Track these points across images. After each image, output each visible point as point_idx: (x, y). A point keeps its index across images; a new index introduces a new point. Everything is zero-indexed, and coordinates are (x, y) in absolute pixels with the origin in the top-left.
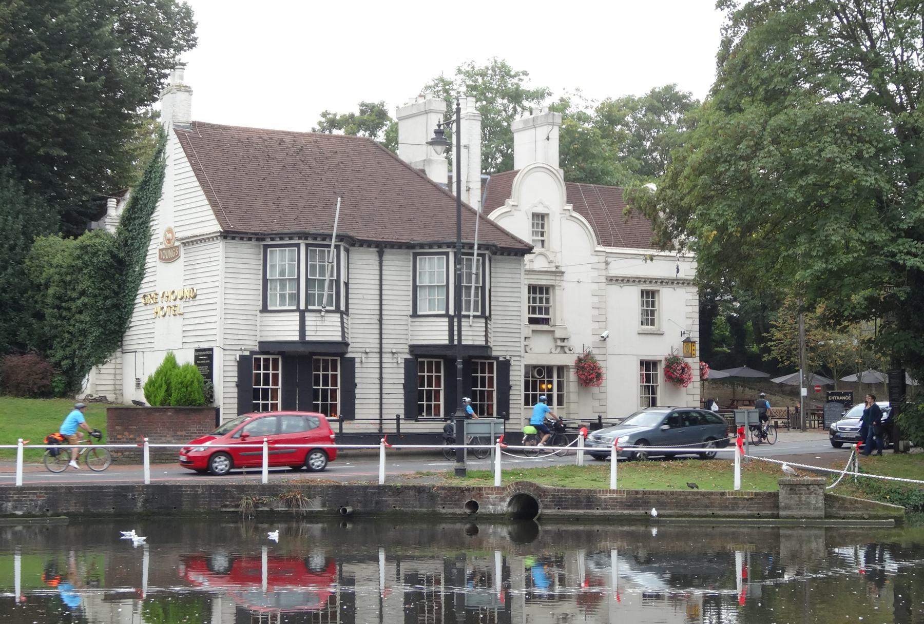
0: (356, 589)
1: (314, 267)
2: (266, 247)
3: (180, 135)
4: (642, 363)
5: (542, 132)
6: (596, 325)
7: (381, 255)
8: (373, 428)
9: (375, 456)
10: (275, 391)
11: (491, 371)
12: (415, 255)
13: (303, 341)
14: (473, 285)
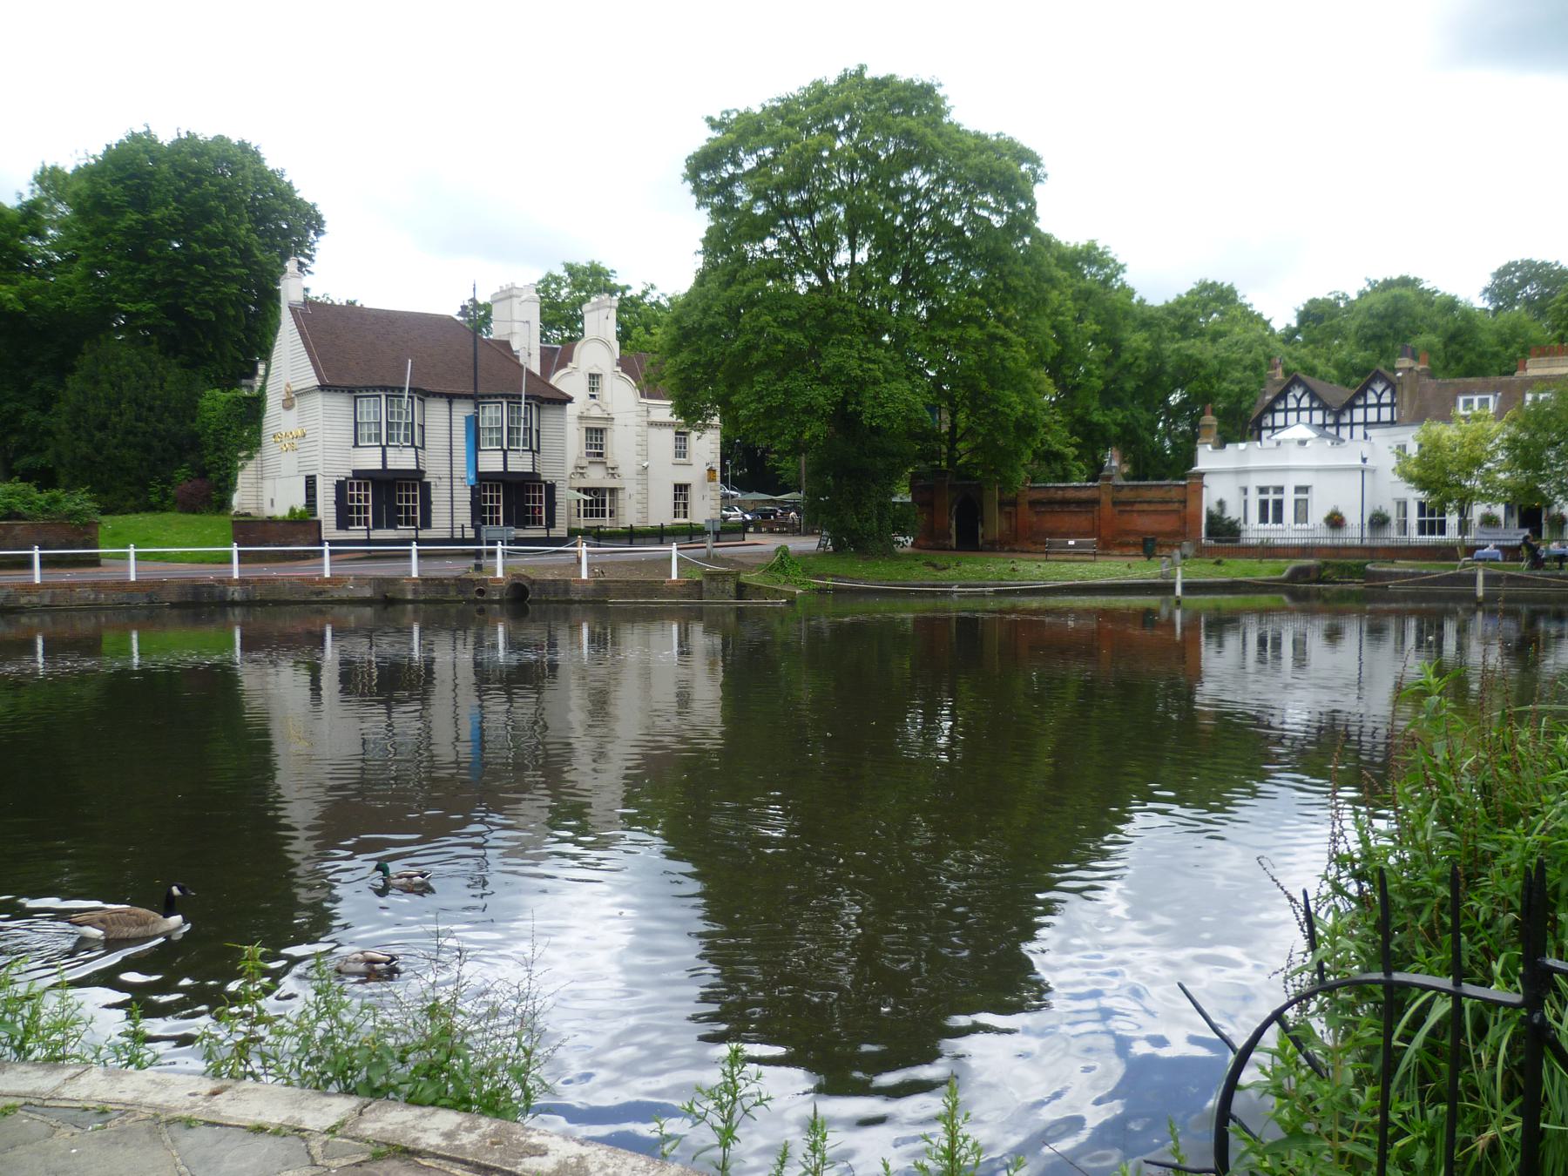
0: (435, 654)
1: (392, 413)
2: (356, 397)
3: (293, 310)
4: (676, 486)
5: (604, 312)
6: (640, 458)
7: (450, 403)
8: (446, 535)
9: (407, 556)
10: (366, 508)
11: (540, 492)
12: (356, 397)
13: (385, 469)
14: (403, 422)
